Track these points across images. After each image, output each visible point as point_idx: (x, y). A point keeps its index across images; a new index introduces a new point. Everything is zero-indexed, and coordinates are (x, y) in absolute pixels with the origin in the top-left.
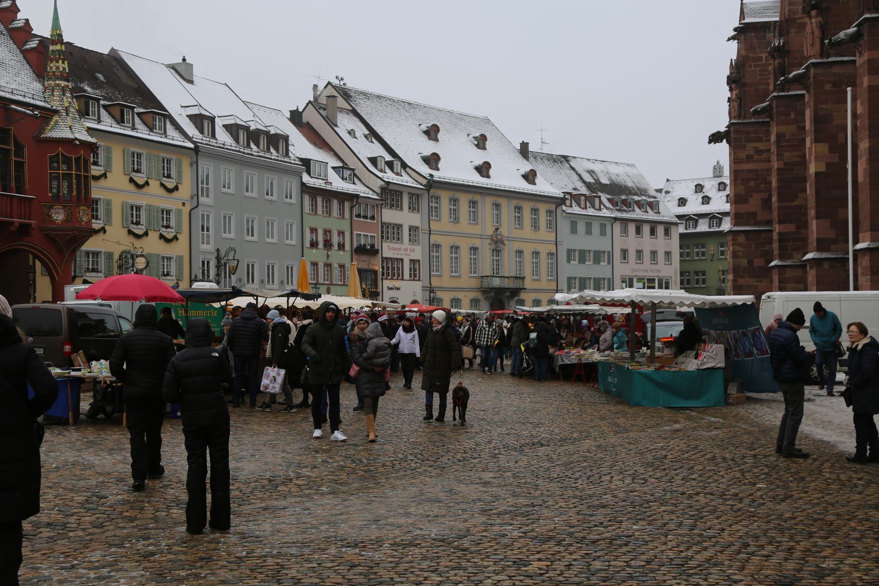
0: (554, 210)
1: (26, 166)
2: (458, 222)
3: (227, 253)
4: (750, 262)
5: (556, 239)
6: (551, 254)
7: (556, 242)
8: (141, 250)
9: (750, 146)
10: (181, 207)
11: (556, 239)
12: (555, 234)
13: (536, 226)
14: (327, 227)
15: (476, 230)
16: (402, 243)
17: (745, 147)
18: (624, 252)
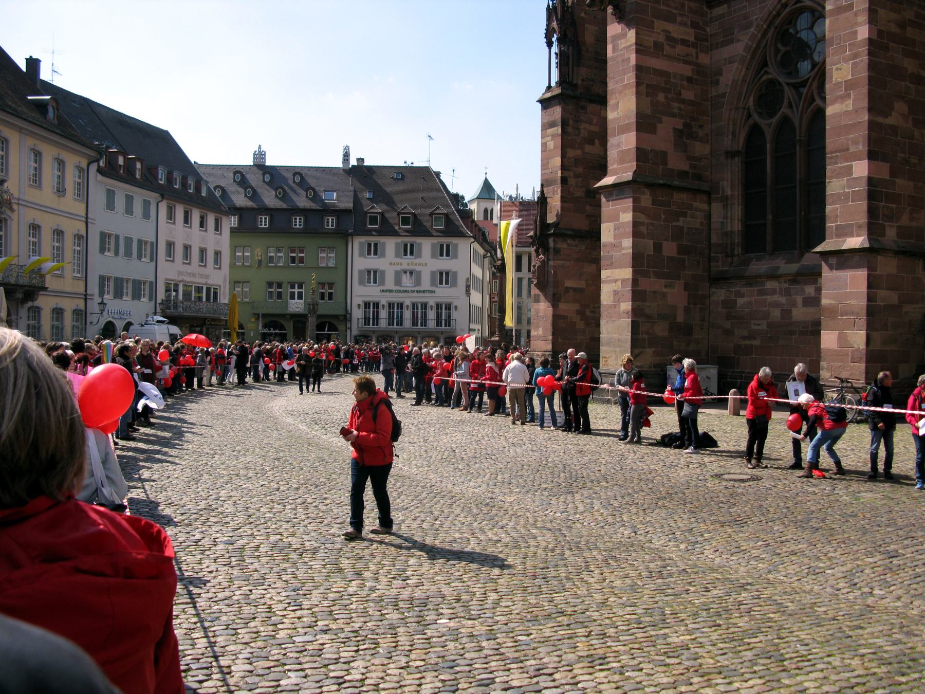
0: (85, 168)
5: (87, 214)
6: (78, 237)
7: (87, 218)
11: (87, 214)
12: (85, 205)
13: (61, 191)
18: (170, 245)
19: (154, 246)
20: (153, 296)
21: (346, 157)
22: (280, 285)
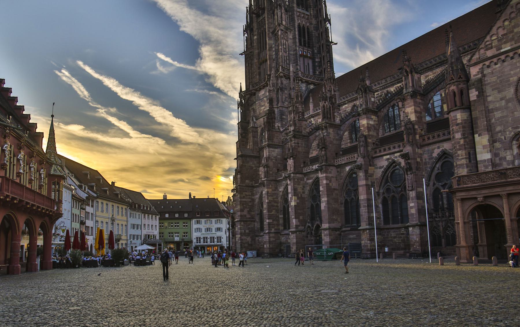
4: (245, 231)
6: (126, 225)
9: (244, 193)
15: (106, 215)
17: (242, 193)
18: (144, 225)
19: (141, 225)
20: (141, 239)
21: (190, 195)
22: (172, 233)
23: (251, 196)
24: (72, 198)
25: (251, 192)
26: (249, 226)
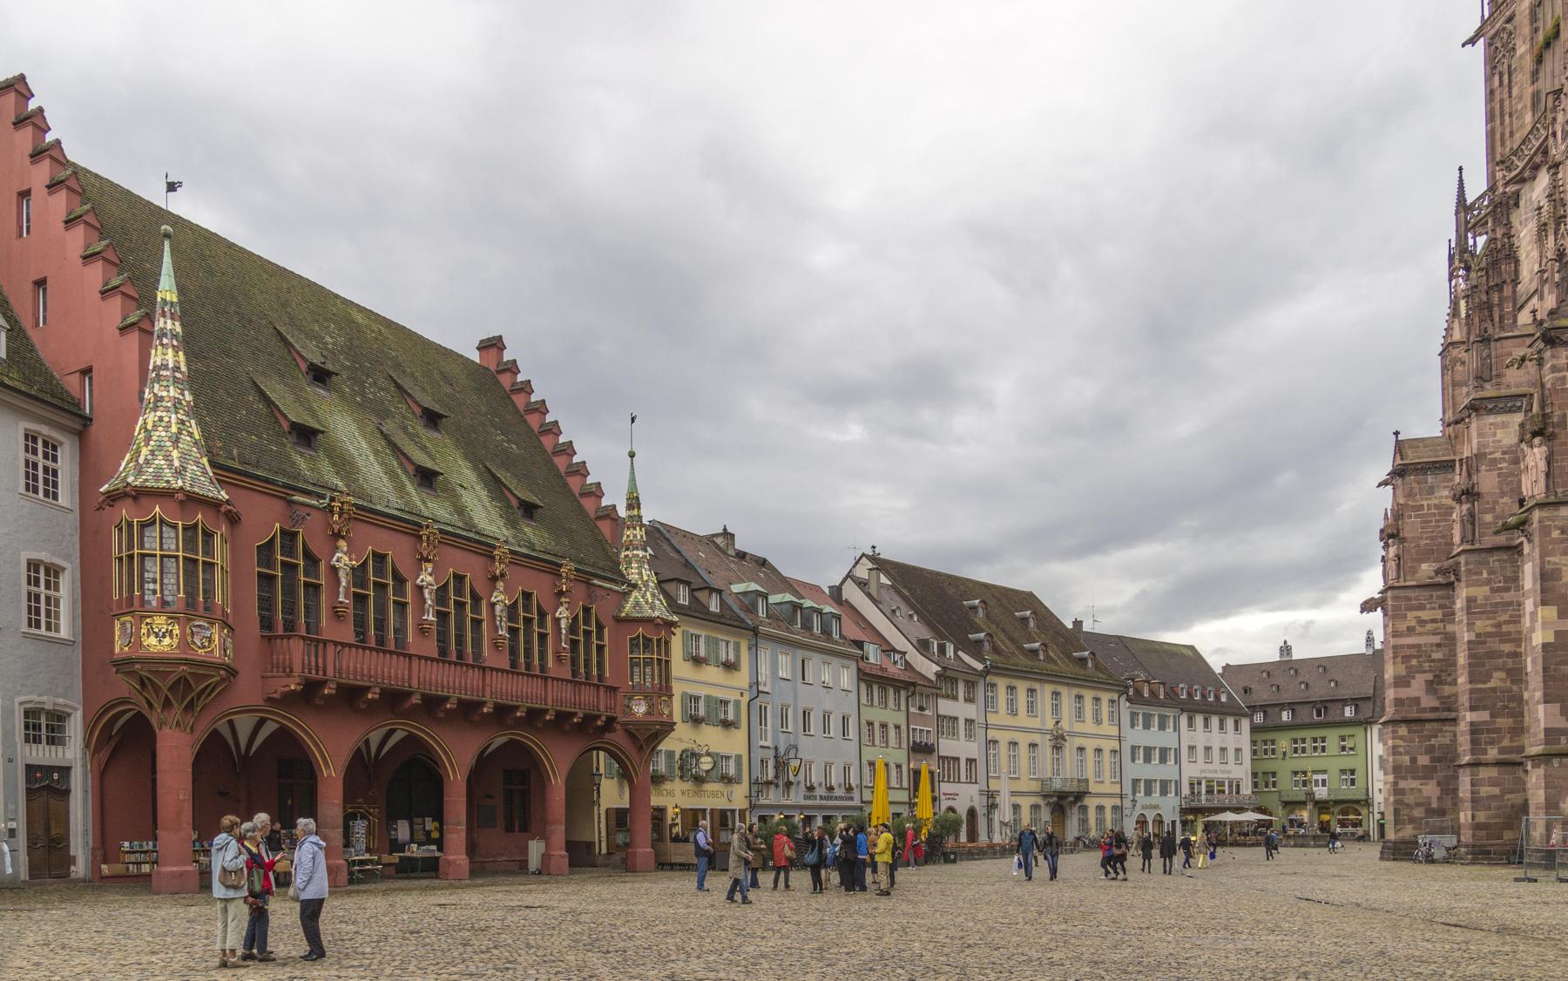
1: (607, 650)
2: (1016, 714)
3: (787, 751)
8: (706, 748)
9: (1411, 615)
10: (739, 698)
13: (1098, 721)
14: (884, 720)
15: (1035, 723)
16: (958, 739)
17: (1405, 616)
18: (1192, 748)
19: (1177, 752)
22: (1305, 773)
23: (1441, 625)
24: (859, 679)
25: (1441, 607)
26: (1433, 741)
